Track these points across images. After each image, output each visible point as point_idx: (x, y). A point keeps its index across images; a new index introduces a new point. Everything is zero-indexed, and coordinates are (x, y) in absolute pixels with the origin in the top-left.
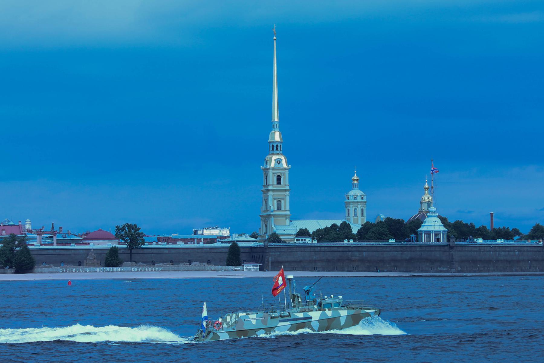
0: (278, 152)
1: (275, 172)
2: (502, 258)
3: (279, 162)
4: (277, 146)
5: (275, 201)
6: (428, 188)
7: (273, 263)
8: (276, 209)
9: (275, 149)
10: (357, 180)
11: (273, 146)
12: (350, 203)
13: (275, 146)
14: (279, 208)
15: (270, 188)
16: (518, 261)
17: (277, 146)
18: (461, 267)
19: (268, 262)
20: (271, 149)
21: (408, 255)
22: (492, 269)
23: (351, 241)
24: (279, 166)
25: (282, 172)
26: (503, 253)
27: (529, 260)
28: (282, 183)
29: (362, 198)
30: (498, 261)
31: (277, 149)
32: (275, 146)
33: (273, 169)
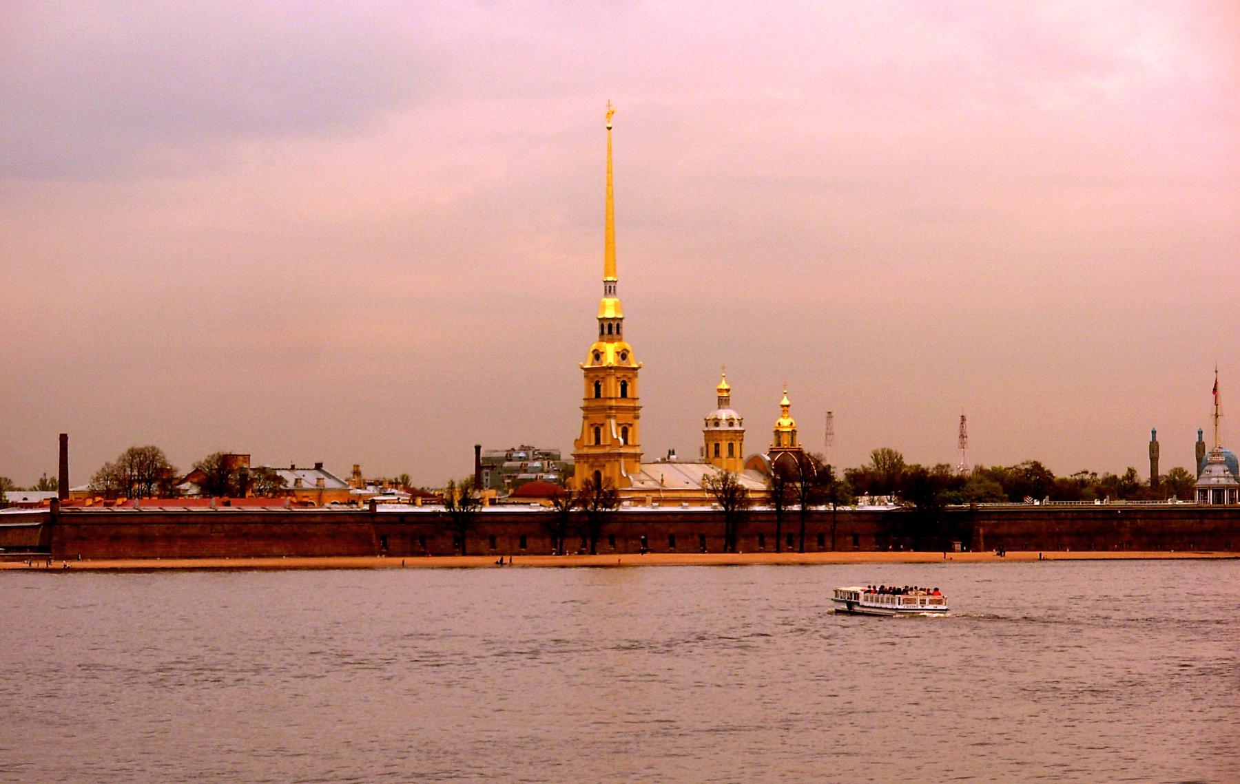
1: (619, 375)
3: (623, 355)
5: (620, 429)
7: (986, 537)
10: (728, 390)
11: (610, 326)
13: (614, 326)
15: (613, 403)
19: (978, 535)
20: (606, 331)
21: (1209, 524)
23: (1046, 501)
24: (624, 364)
25: (630, 375)
28: (629, 395)
32: (614, 326)
33: (617, 369)
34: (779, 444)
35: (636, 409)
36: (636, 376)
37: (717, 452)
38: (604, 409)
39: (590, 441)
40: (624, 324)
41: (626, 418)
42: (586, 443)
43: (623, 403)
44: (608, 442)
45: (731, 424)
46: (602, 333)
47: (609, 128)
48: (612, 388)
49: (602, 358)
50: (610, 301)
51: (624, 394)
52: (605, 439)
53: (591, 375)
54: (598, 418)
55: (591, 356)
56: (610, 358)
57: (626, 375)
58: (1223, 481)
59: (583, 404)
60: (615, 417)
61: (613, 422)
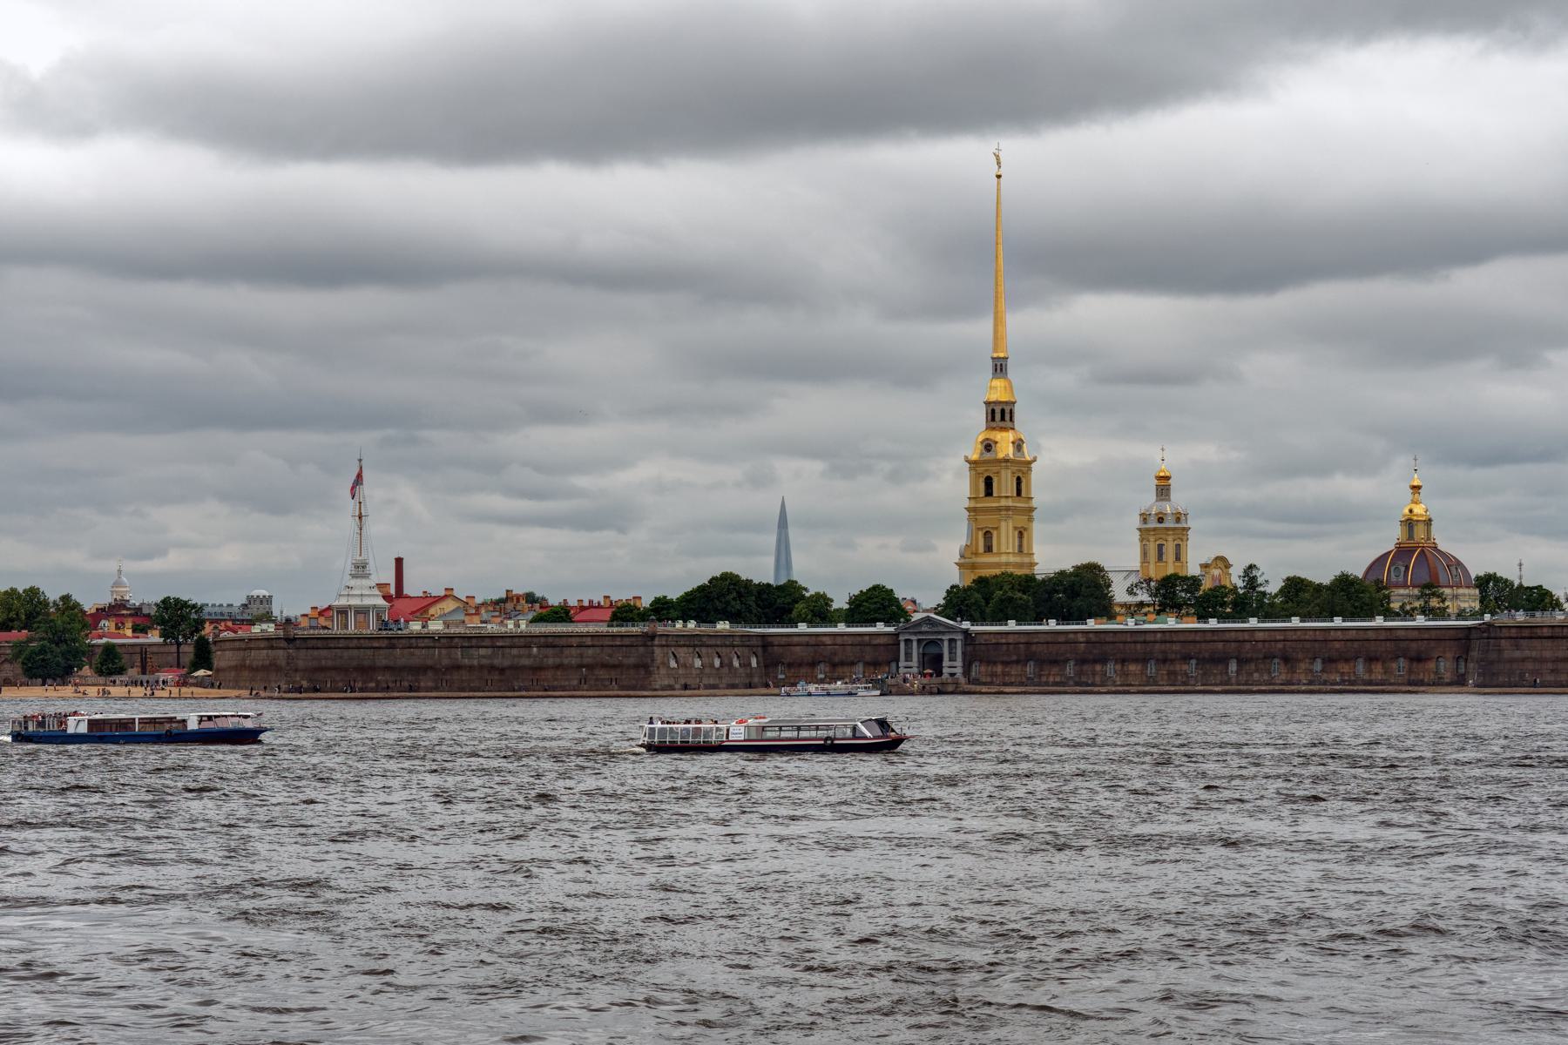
0: (994, 424)
1: (980, 469)
2: (475, 662)
5: (981, 534)
6: (1419, 487)
8: (981, 549)
9: (1007, 417)
14: (989, 549)
16: (537, 669)
18: (310, 680)
22: (430, 684)
24: (988, 456)
25: (995, 469)
26: (482, 651)
27: (580, 666)
29: (1161, 520)
30: (458, 667)
31: (993, 419)
34: (1411, 537)
35: (1032, 509)
40: (1017, 410)
43: (990, 503)
54: (987, 521)
56: (1005, 449)
57: (1021, 472)
58: (367, 602)
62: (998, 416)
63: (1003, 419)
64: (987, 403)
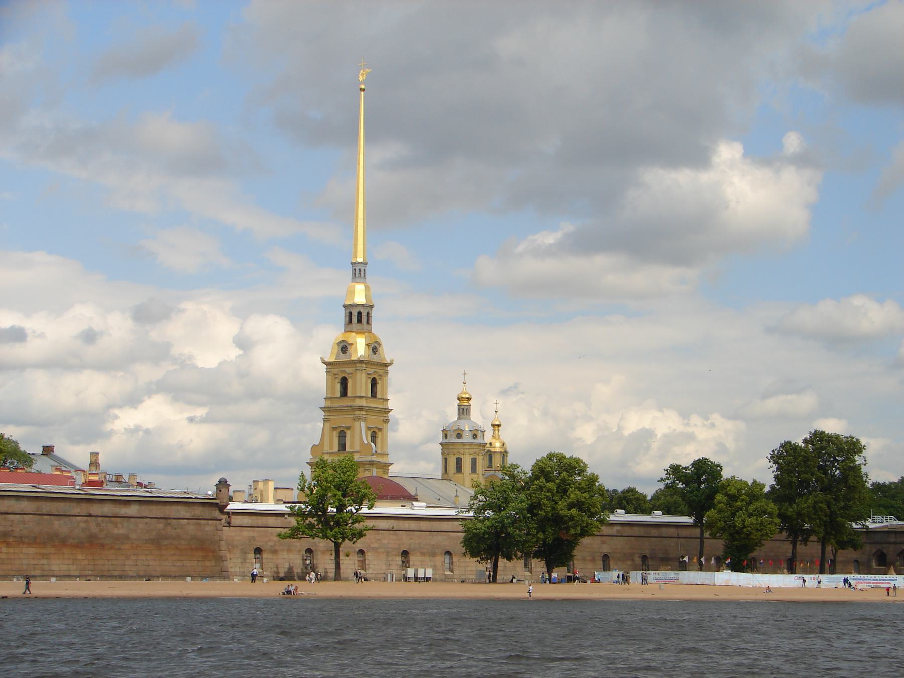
1: (371, 371)
3: (374, 347)
4: (368, 314)
5: (369, 433)
6: (499, 426)
10: (469, 399)
11: (359, 314)
12: (463, 444)
15: (363, 402)
17: (368, 314)
20: (355, 319)
24: (375, 358)
25: (381, 372)
28: (379, 395)
36: (386, 373)
37: (459, 468)
38: (352, 409)
39: (331, 447)
41: (375, 421)
42: (326, 449)
43: (373, 404)
44: (357, 448)
45: (475, 437)
46: (350, 321)
47: (363, 90)
48: (360, 385)
49: (351, 349)
50: (359, 288)
51: (374, 394)
52: (352, 446)
53: (336, 370)
54: (343, 420)
55: (337, 349)
59: (323, 404)
60: (365, 420)
61: (363, 424)
62: (355, 319)
63: (359, 321)
64: (345, 306)
